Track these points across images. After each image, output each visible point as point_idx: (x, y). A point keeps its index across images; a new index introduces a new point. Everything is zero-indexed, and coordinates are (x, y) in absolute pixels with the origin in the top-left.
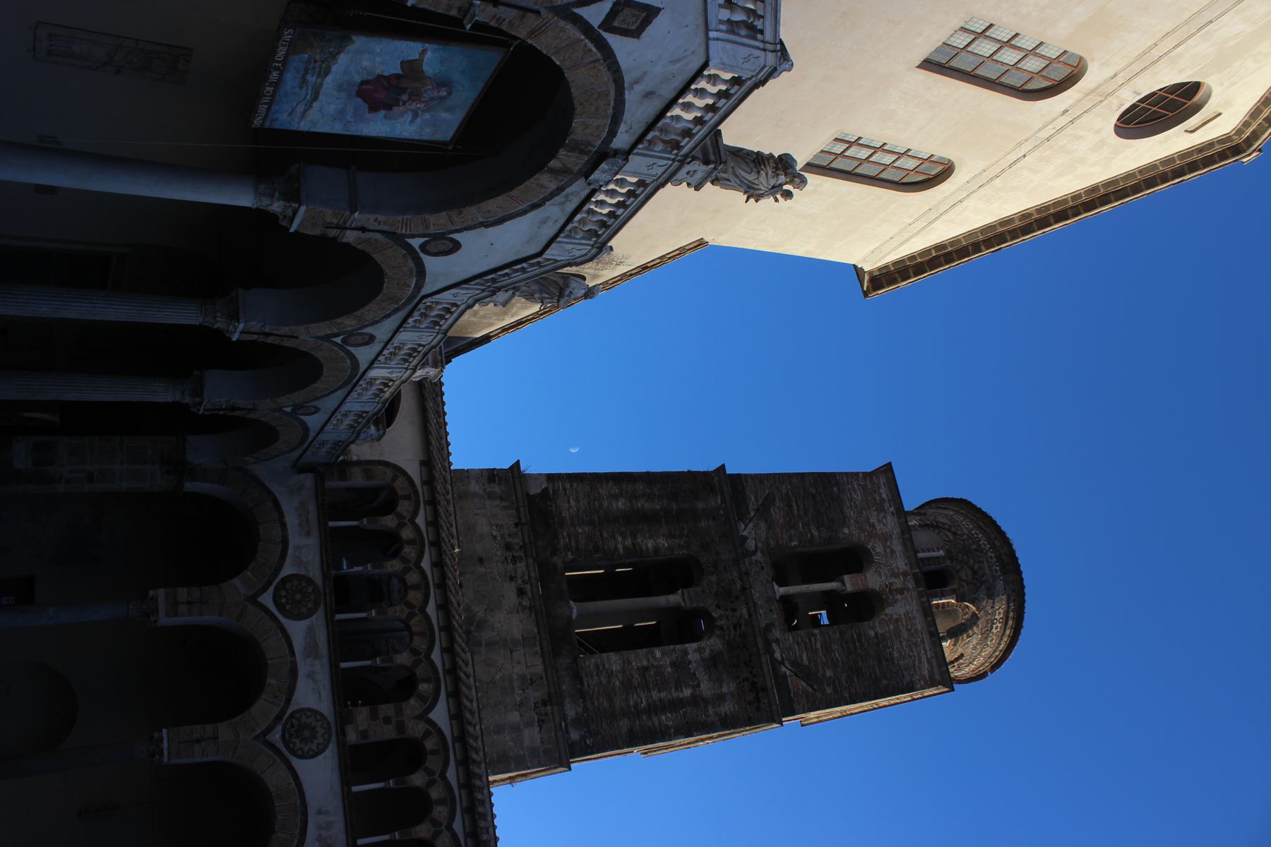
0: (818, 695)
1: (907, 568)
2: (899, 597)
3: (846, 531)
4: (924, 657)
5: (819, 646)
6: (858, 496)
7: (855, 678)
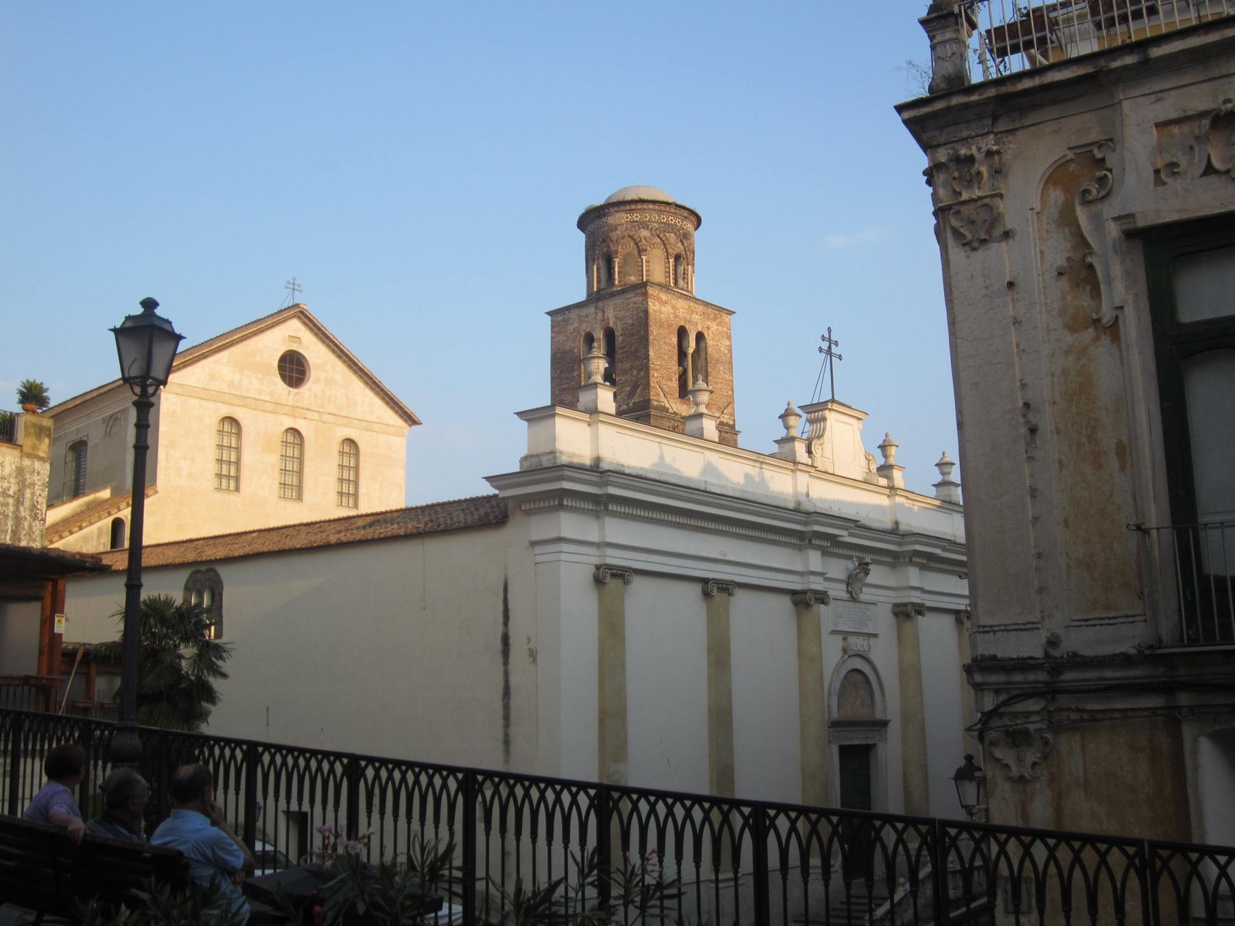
0: (643, 381)
1: (594, 305)
2: (606, 315)
3: (576, 351)
4: (634, 300)
5: (623, 378)
6: (562, 338)
7: (639, 354)
